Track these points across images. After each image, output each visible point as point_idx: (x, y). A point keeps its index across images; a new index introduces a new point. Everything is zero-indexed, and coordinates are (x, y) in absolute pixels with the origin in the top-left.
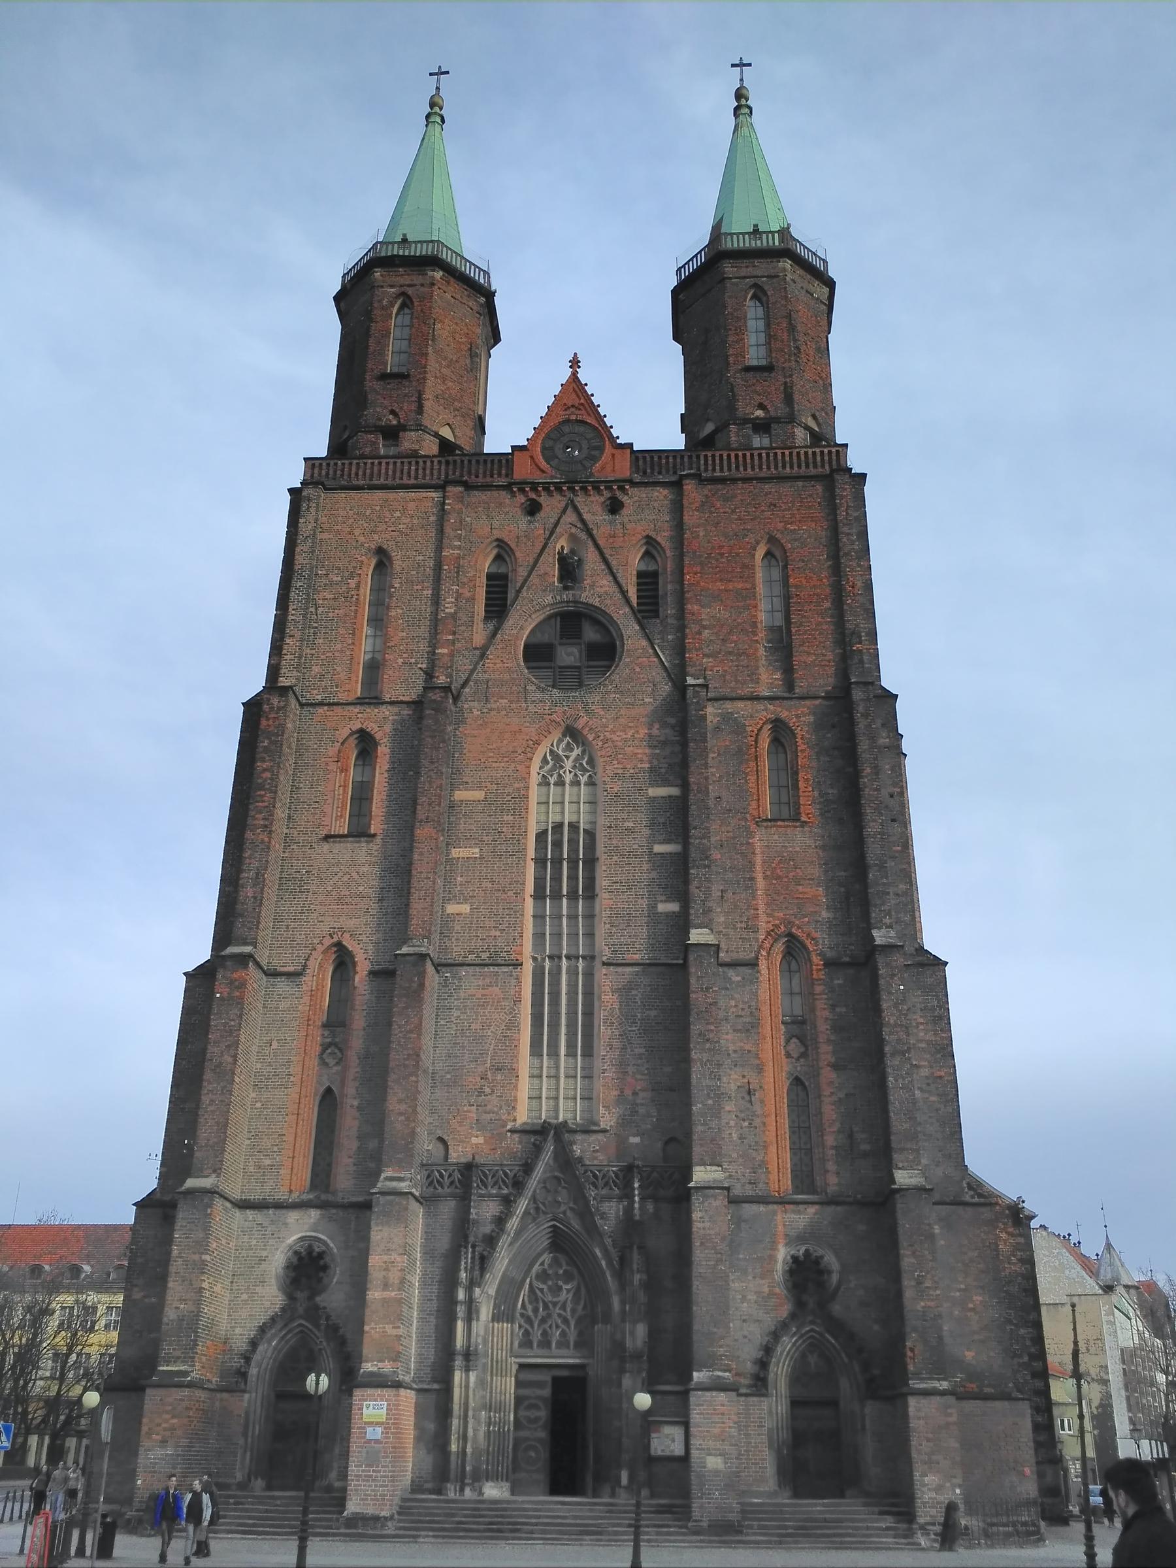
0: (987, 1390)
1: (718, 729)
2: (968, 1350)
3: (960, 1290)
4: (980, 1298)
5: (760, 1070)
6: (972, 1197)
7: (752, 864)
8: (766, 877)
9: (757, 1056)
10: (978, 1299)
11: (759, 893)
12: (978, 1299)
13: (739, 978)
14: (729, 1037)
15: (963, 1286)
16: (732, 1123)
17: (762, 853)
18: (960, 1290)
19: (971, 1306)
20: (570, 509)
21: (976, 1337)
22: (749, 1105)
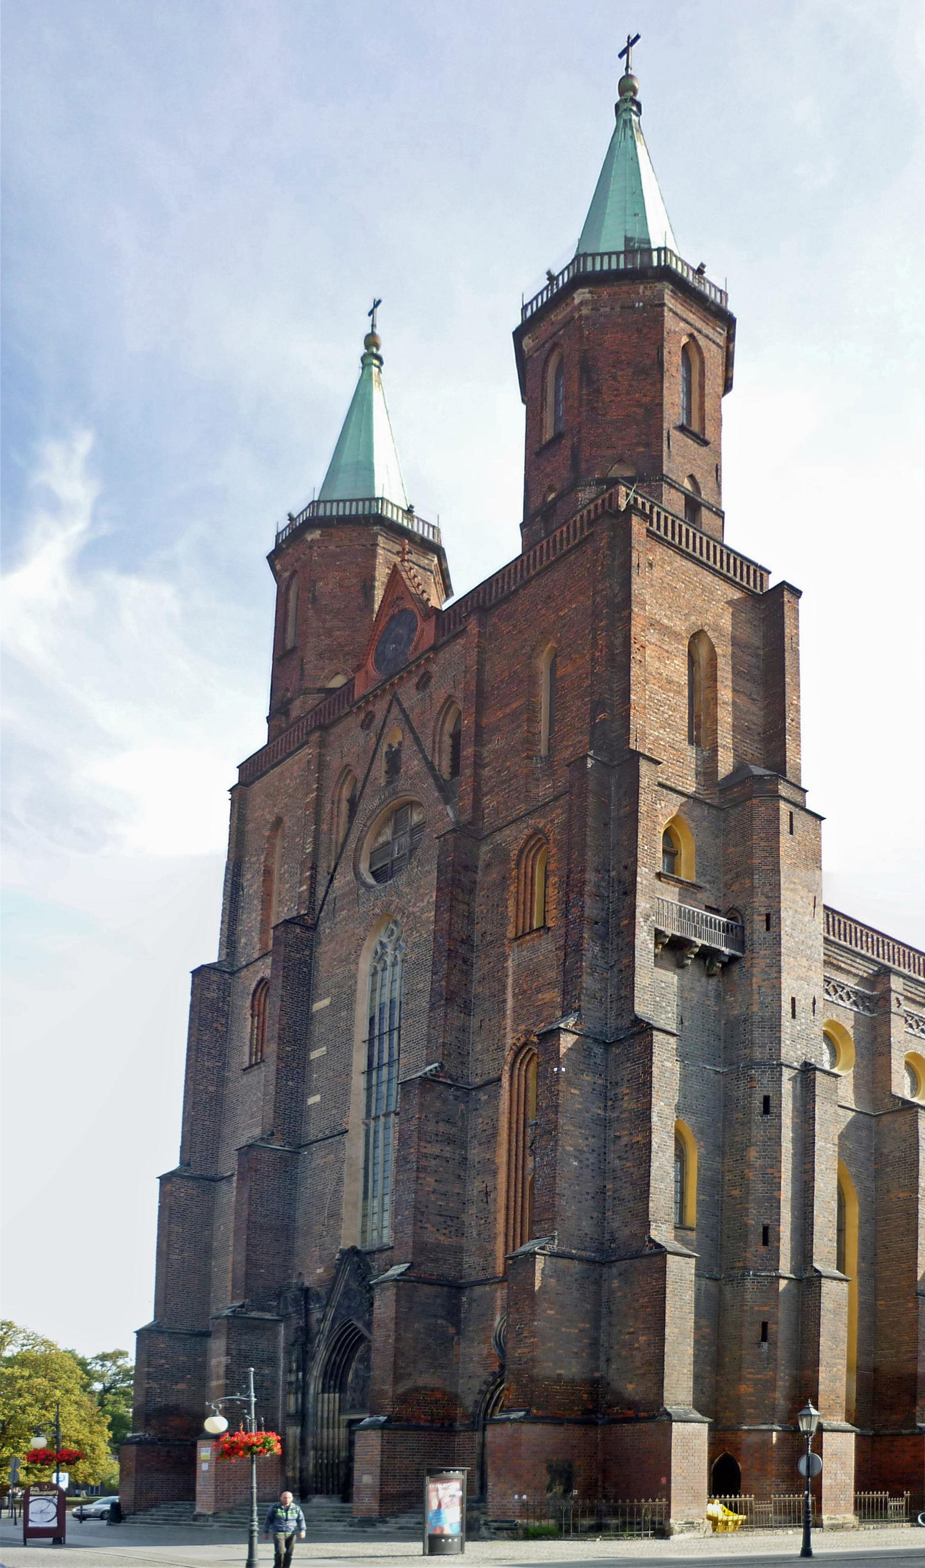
0: (642, 1414)
1: (488, 866)
2: (630, 1383)
3: (629, 1333)
4: (644, 1338)
5: (495, 1173)
6: (651, 1248)
7: (505, 987)
8: (515, 995)
9: (494, 1163)
10: (642, 1339)
11: (508, 1012)
12: (642, 1339)
13: (486, 1097)
14: (476, 1151)
15: (632, 1330)
16: (473, 1223)
17: (514, 973)
18: (629, 1333)
19: (636, 1345)
20: (395, 704)
21: (637, 1372)
22: (485, 1205)
